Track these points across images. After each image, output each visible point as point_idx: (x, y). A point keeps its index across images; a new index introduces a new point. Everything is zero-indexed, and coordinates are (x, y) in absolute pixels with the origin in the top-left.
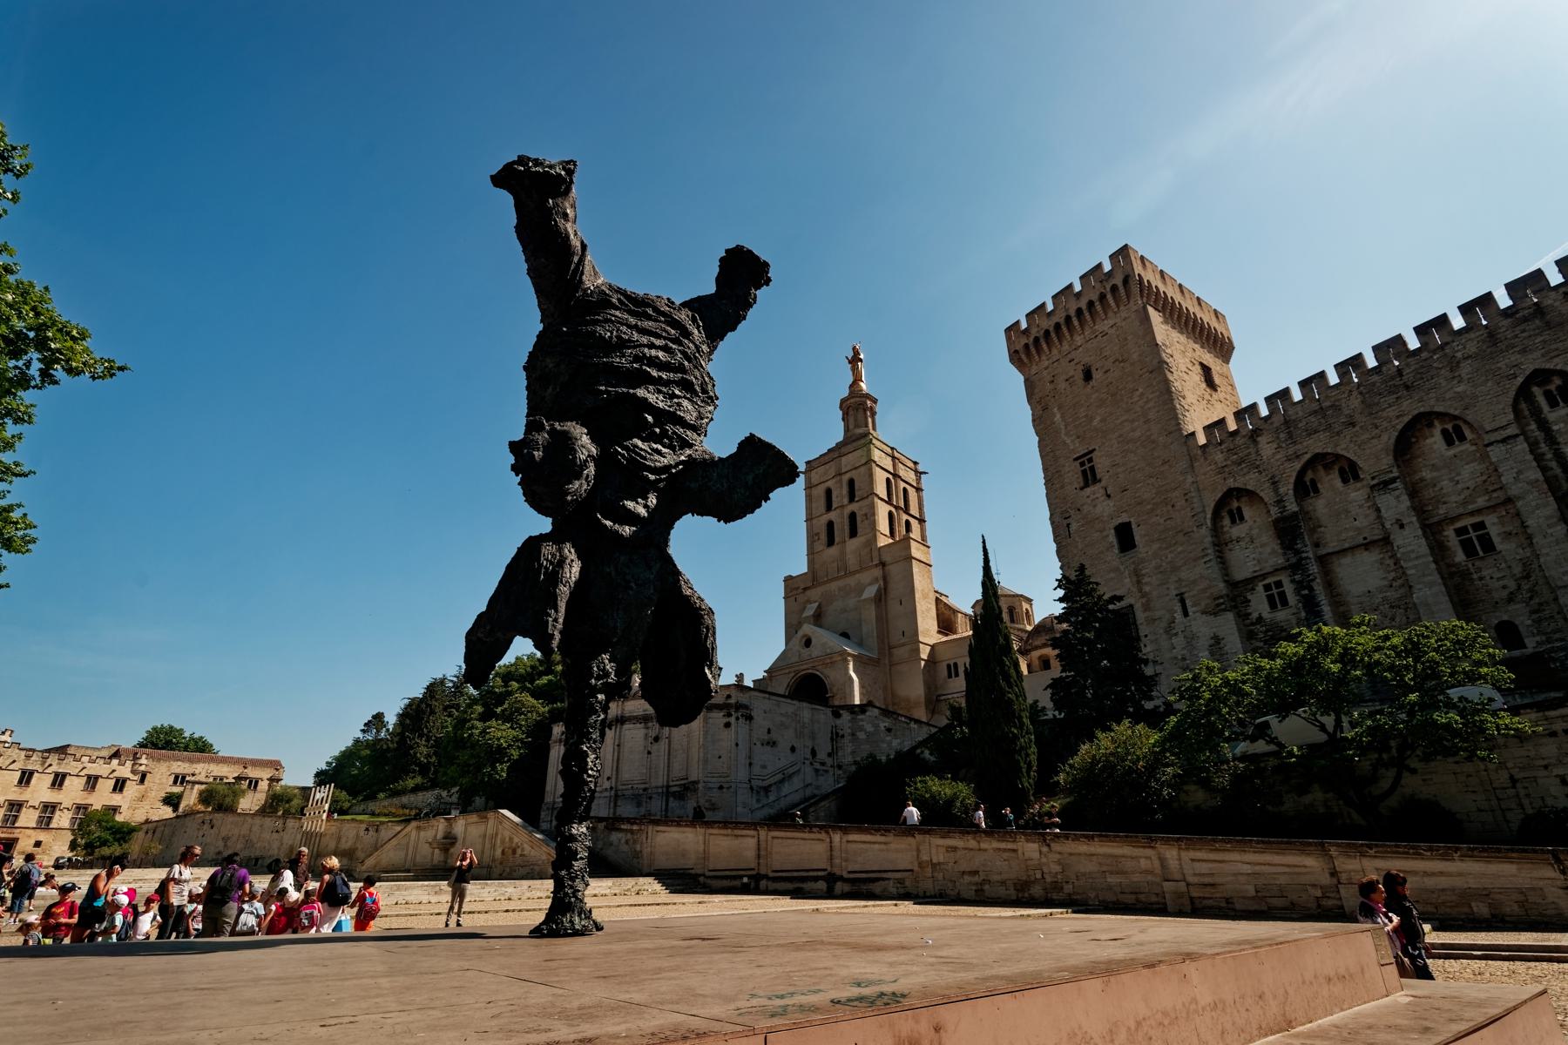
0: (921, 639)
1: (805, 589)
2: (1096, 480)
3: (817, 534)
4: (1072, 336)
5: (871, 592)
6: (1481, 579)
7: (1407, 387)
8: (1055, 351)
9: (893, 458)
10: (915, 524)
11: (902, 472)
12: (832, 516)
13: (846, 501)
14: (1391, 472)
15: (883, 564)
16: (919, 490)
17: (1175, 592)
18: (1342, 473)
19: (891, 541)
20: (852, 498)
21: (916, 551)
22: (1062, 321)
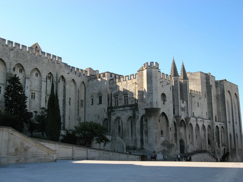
6: (32, 103)
7: (37, 62)
14: (29, 76)
18: (20, 69)
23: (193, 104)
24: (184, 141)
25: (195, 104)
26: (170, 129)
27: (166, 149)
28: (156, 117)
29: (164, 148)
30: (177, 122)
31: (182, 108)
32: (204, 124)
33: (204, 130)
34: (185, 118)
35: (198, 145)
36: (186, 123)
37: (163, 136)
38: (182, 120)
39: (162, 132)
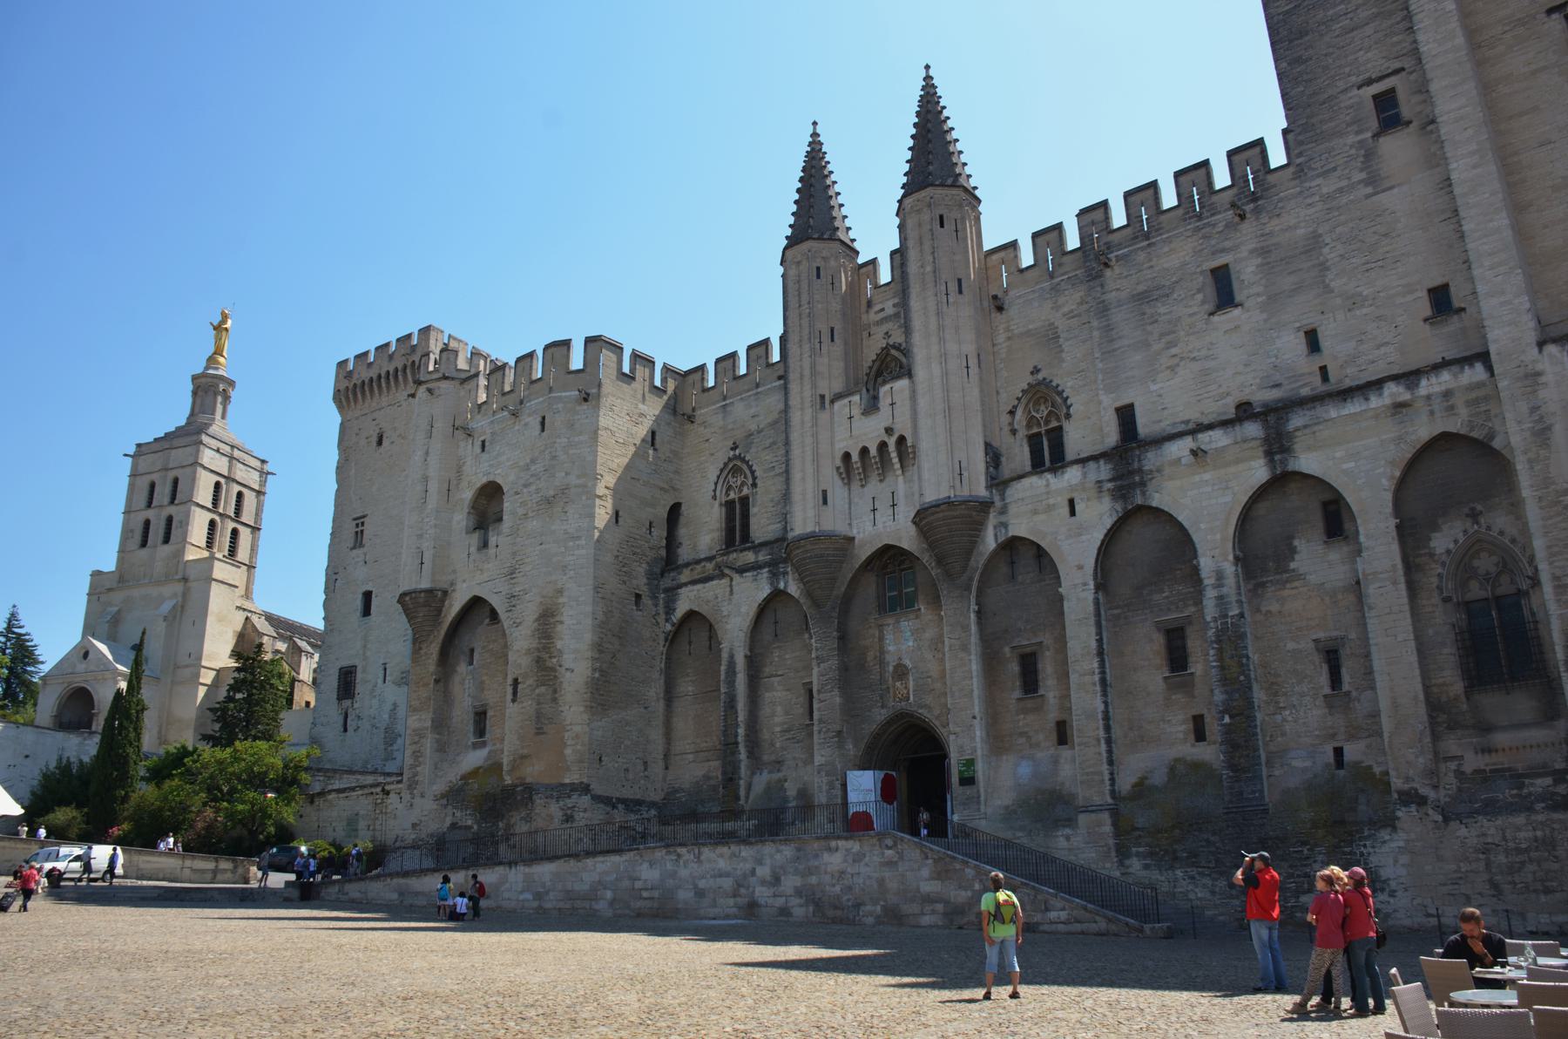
0: (204, 663)
1: (110, 590)
2: (362, 545)
3: (132, 531)
4: (380, 395)
5: (166, 607)
8: (366, 405)
9: (231, 458)
10: (245, 534)
11: (241, 473)
12: (150, 514)
13: (166, 500)
15: (185, 580)
16: (260, 493)
17: (382, 662)
19: (206, 554)
20: (172, 501)
21: (221, 570)
22: (375, 377)
23: (1108, 329)
24: (942, 732)
25: (1162, 310)
26: (510, 690)
27: (469, 823)
28: (424, 646)
29: (458, 814)
30: (809, 594)
31: (864, 451)
32: (1307, 461)
33: (1347, 526)
34: (914, 522)
35: (1200, 735)
36: (940, 561)
37: (484, 744)
38: (889, 558)
39: (480, 717)
